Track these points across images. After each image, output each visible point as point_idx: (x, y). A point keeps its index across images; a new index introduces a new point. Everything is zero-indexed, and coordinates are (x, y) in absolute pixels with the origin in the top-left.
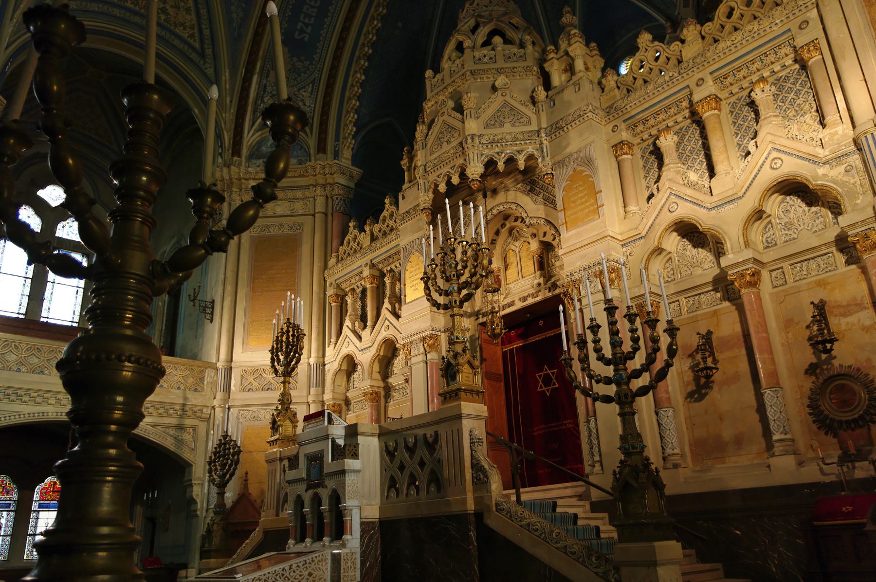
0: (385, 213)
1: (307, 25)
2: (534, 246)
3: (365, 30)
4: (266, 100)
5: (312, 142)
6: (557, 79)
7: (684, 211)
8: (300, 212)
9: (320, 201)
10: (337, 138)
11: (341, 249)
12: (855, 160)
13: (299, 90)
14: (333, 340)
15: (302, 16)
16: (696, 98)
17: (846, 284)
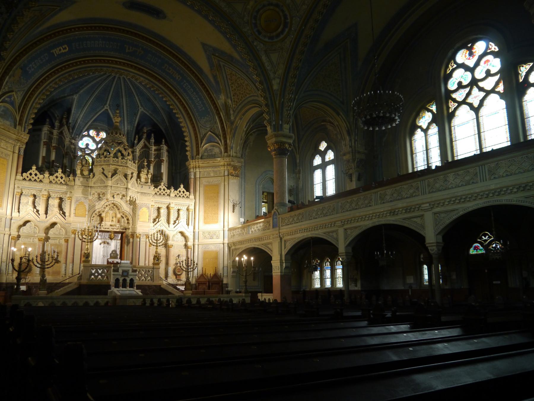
0: (56, 174)
1: (33, 67)
2: (119, 216)
3: (51, 85)
4: (6, 88)
5: (18, 119)
6: (143, 180)
7: (163, 228)
8: (9, 149)
9: (17, 148)
10: (26, 122)
11: (24, 174)
12: (192, 233)
13: (18, 91)
14: (16, 210)
15: (33, 63)
16: (171, 206)
17: (183, 252)
